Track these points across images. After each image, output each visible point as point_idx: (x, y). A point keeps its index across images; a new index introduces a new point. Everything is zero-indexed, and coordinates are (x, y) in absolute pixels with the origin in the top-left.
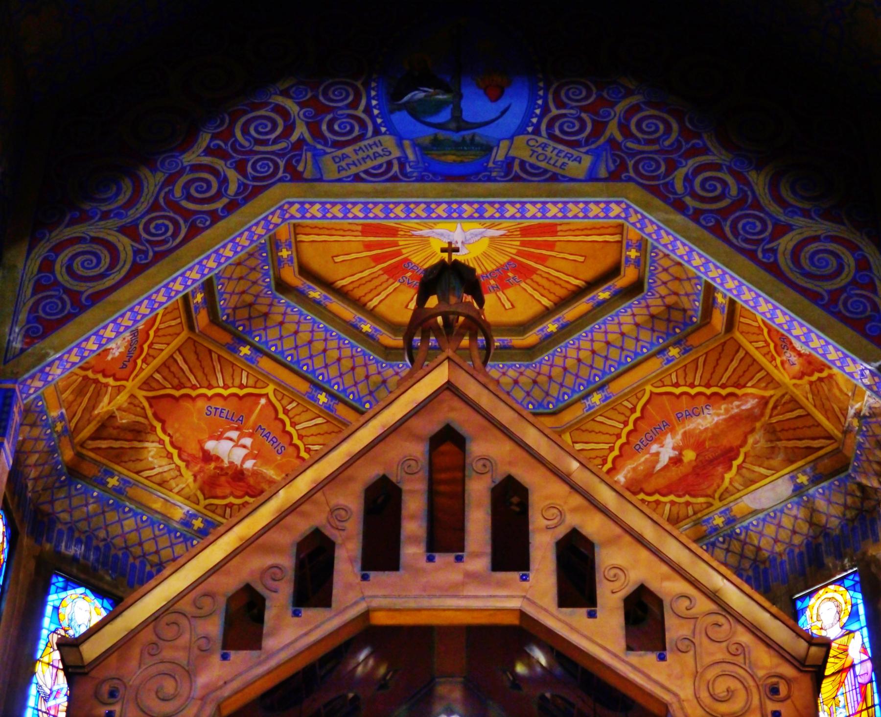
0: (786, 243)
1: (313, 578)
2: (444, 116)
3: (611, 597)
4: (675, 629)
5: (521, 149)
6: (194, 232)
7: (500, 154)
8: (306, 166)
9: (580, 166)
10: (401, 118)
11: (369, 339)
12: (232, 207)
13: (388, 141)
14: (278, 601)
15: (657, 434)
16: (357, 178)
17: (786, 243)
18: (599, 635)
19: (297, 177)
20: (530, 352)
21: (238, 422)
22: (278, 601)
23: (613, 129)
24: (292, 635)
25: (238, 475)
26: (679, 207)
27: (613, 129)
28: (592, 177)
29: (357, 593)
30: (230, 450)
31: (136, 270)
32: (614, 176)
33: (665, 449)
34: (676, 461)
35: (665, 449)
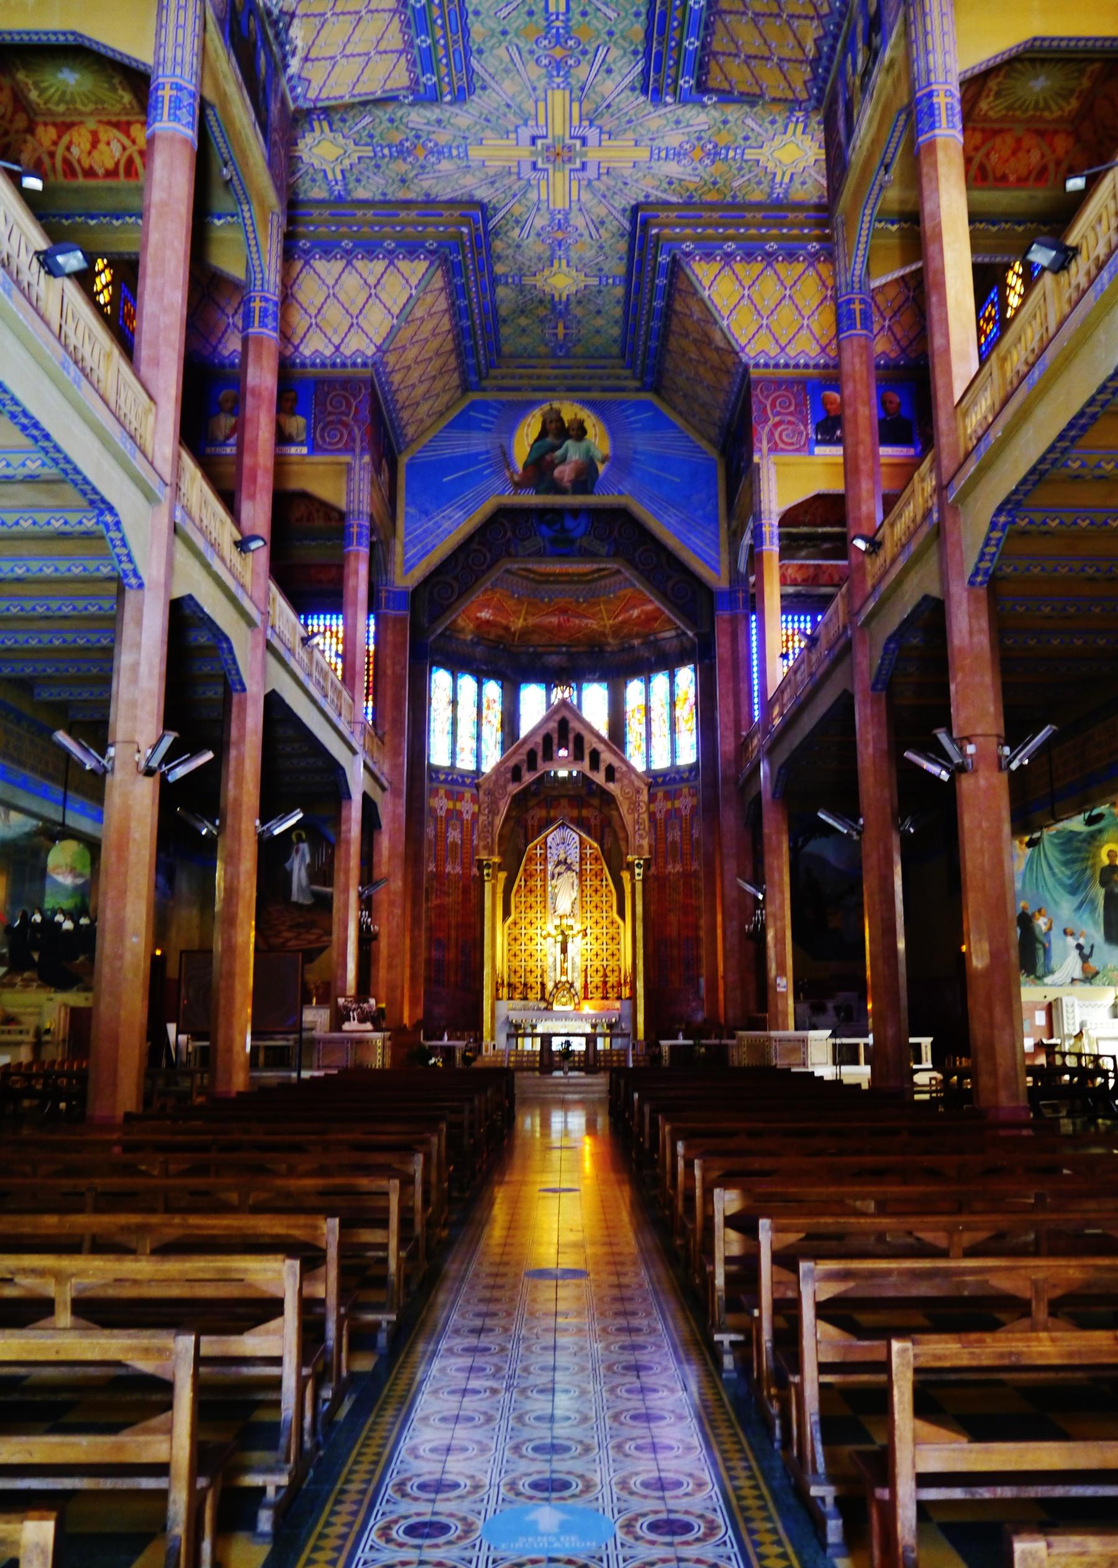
0: (670, 584)
1: (532, 765)
2: (558, 527)
3: (602, 767)
4: (617, 775)
5: (584, 542)
6: (477, 579)
7: (578, 543)
8: (512, 550)
9: (603, 551)
10: (544, 529)
11: (532, 580)
12: (489, 568)
13: (539, 539)
14: (524, 768)
15: (635, 607)
16: (529, 555)
17: (670, 584)
18: (599, 778)
19: (510, 555)
20: (589, 582)
21: (488, 607)
22: (524, 768)
23: (616, 533)
24: (528, 778)
25: (488, 622)
26: (636, 568)
27: (616, 533)
28: (608, 555)
29: (542, 767)
30: (485, 615)
31: (460, 596)
32: (615, 555)
33: (635, 613)
34: (639, 617)
35: (635, 613)
